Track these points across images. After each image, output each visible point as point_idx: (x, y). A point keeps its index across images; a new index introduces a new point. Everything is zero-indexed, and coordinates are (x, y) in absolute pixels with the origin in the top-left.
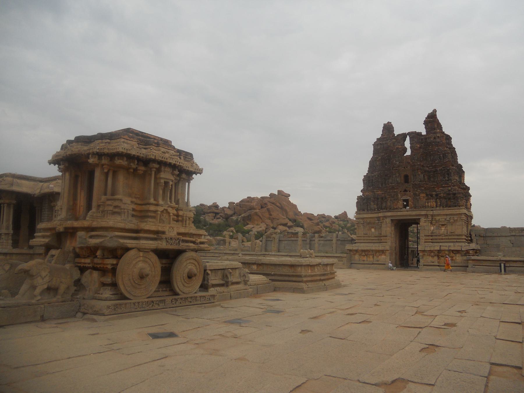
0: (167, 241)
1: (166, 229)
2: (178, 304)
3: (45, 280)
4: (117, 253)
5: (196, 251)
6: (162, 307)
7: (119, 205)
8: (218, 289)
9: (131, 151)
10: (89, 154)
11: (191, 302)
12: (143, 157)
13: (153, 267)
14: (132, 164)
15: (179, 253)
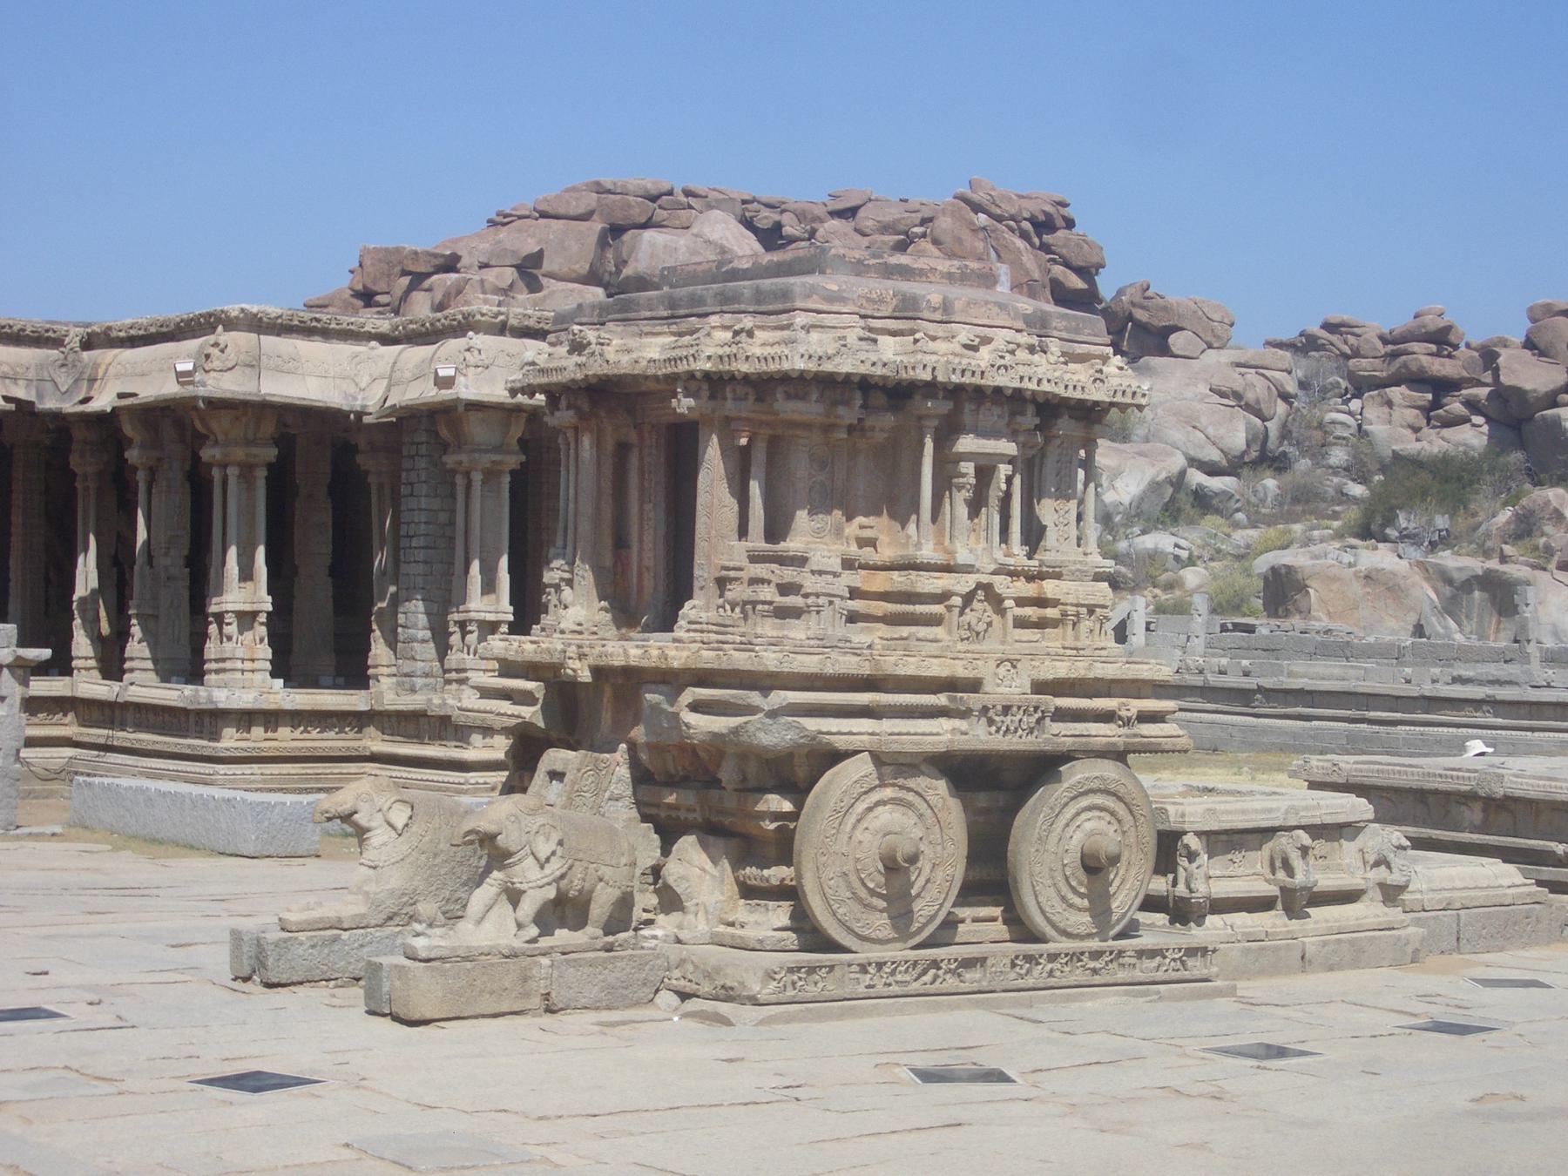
0: (991, 722)
1: (985, 670)
2: (1038, 975)
3: (548, 870)
4: (796, 773)
5: (1119, 755)
6: (975, 987)
7: (798, 580)
8: (1241, 919)
9: (837, 360)
10: (672, 379)
11: (1095, 971)
12: (884, 377)
13: (935, 827)
14: (841, 410)
15: (1042, 768)
